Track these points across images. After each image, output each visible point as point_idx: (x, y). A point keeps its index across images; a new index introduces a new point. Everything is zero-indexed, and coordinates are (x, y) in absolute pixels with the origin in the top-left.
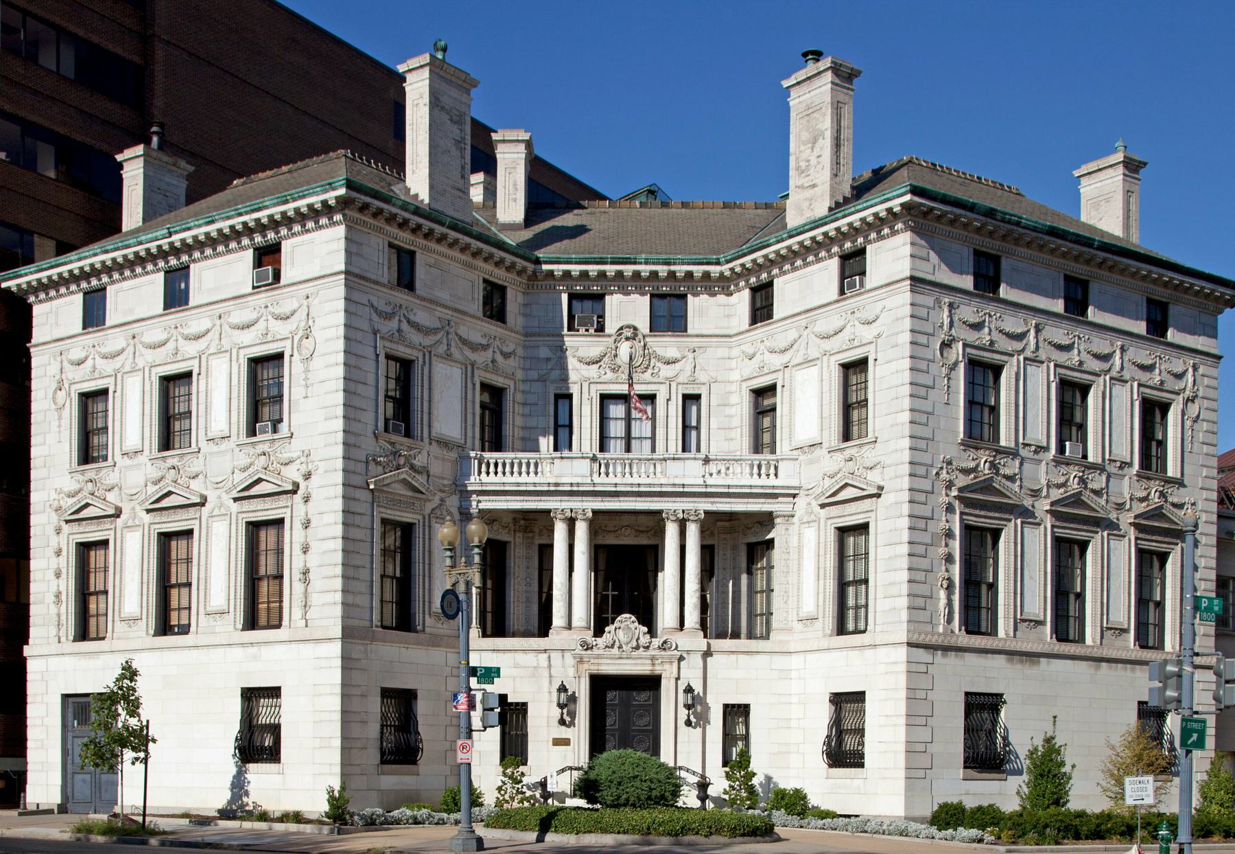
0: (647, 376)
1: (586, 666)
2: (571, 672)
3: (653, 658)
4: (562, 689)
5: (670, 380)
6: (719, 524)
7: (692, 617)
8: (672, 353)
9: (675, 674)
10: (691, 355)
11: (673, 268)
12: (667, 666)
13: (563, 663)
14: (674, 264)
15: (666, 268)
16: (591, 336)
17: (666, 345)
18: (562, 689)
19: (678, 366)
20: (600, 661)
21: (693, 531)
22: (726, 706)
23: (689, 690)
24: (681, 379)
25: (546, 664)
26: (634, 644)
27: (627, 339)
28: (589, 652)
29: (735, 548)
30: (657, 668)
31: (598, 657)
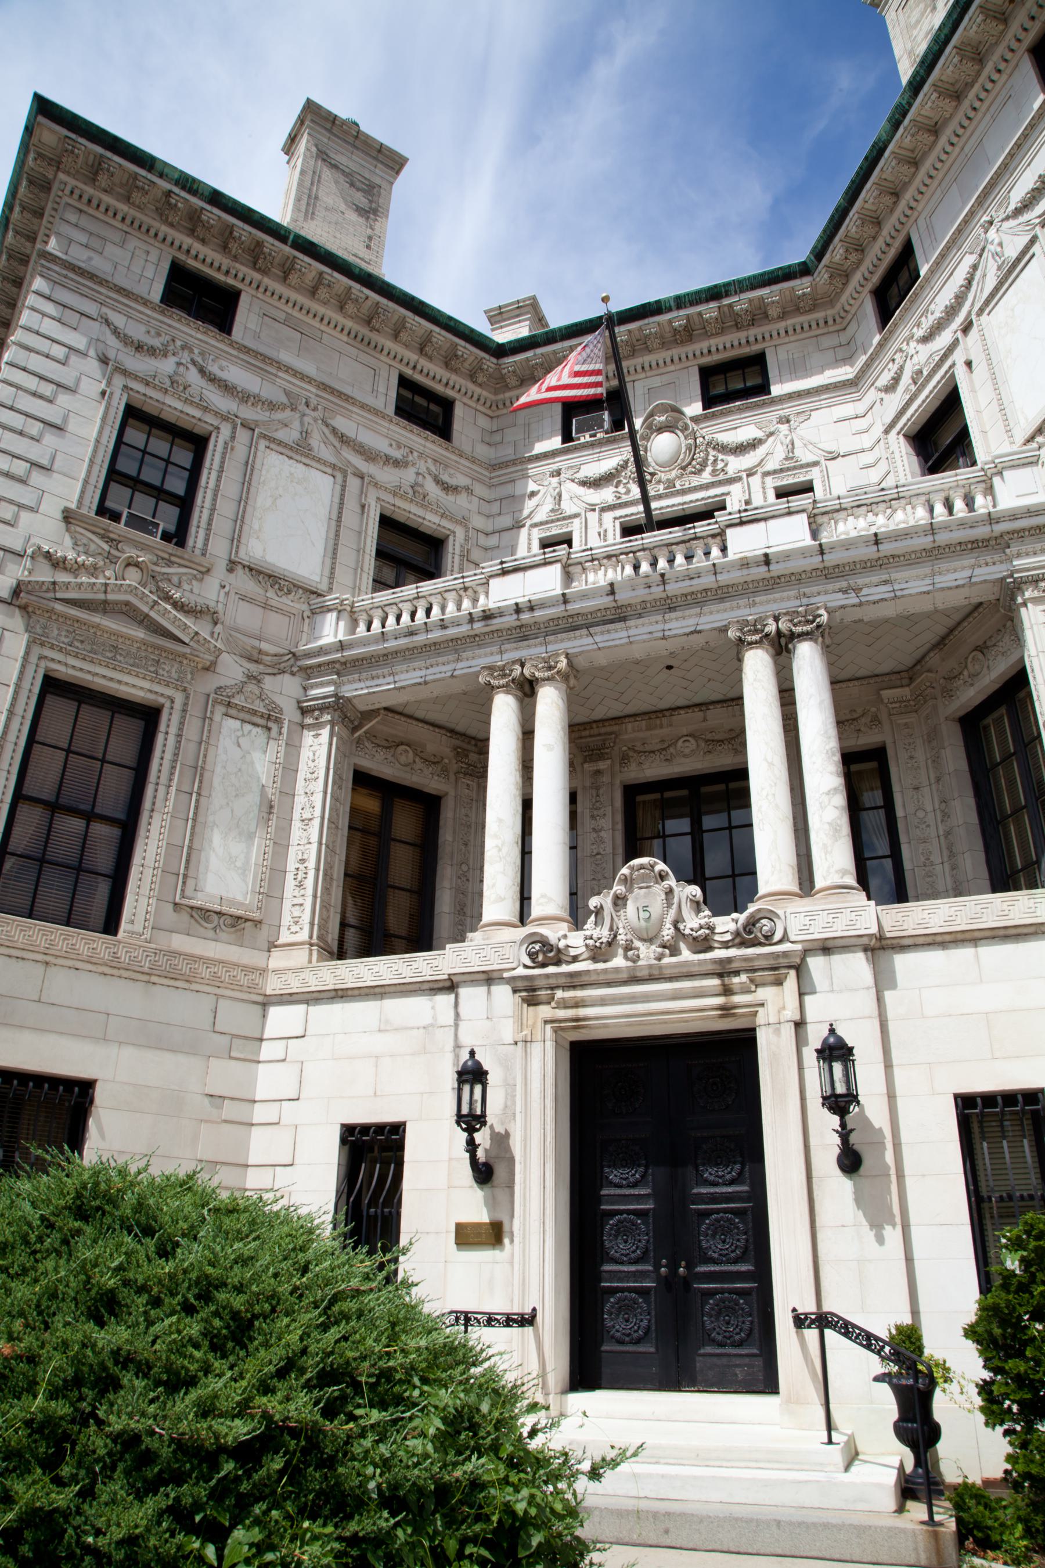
0: (706, 477)
1: (545, 1011)
2: (508, 1031)
3: (724, 971)
4: (472, 1074)
5: (750, 473)
6: (886, 694)
8: (746, 432)
9: (791, 1012)
10: (784, 428)
11: (726, 301)
12: (764, 993)
13: (489, 1007)
14: (727, 295)
15: (713, 305)
16: (600, 443)
17: (739, 426)
18: (472, 1074)
19: (761, 451)
21: (808, 663)
22: (965, 1103)
23: (836, 1051)
24: (771, 465)
25: (449, 1018)
26: (668, 932)
27: (660, 430)
28: (551, 969)
29: (932, 736)
30: (737, 999)
31: (574, 982)
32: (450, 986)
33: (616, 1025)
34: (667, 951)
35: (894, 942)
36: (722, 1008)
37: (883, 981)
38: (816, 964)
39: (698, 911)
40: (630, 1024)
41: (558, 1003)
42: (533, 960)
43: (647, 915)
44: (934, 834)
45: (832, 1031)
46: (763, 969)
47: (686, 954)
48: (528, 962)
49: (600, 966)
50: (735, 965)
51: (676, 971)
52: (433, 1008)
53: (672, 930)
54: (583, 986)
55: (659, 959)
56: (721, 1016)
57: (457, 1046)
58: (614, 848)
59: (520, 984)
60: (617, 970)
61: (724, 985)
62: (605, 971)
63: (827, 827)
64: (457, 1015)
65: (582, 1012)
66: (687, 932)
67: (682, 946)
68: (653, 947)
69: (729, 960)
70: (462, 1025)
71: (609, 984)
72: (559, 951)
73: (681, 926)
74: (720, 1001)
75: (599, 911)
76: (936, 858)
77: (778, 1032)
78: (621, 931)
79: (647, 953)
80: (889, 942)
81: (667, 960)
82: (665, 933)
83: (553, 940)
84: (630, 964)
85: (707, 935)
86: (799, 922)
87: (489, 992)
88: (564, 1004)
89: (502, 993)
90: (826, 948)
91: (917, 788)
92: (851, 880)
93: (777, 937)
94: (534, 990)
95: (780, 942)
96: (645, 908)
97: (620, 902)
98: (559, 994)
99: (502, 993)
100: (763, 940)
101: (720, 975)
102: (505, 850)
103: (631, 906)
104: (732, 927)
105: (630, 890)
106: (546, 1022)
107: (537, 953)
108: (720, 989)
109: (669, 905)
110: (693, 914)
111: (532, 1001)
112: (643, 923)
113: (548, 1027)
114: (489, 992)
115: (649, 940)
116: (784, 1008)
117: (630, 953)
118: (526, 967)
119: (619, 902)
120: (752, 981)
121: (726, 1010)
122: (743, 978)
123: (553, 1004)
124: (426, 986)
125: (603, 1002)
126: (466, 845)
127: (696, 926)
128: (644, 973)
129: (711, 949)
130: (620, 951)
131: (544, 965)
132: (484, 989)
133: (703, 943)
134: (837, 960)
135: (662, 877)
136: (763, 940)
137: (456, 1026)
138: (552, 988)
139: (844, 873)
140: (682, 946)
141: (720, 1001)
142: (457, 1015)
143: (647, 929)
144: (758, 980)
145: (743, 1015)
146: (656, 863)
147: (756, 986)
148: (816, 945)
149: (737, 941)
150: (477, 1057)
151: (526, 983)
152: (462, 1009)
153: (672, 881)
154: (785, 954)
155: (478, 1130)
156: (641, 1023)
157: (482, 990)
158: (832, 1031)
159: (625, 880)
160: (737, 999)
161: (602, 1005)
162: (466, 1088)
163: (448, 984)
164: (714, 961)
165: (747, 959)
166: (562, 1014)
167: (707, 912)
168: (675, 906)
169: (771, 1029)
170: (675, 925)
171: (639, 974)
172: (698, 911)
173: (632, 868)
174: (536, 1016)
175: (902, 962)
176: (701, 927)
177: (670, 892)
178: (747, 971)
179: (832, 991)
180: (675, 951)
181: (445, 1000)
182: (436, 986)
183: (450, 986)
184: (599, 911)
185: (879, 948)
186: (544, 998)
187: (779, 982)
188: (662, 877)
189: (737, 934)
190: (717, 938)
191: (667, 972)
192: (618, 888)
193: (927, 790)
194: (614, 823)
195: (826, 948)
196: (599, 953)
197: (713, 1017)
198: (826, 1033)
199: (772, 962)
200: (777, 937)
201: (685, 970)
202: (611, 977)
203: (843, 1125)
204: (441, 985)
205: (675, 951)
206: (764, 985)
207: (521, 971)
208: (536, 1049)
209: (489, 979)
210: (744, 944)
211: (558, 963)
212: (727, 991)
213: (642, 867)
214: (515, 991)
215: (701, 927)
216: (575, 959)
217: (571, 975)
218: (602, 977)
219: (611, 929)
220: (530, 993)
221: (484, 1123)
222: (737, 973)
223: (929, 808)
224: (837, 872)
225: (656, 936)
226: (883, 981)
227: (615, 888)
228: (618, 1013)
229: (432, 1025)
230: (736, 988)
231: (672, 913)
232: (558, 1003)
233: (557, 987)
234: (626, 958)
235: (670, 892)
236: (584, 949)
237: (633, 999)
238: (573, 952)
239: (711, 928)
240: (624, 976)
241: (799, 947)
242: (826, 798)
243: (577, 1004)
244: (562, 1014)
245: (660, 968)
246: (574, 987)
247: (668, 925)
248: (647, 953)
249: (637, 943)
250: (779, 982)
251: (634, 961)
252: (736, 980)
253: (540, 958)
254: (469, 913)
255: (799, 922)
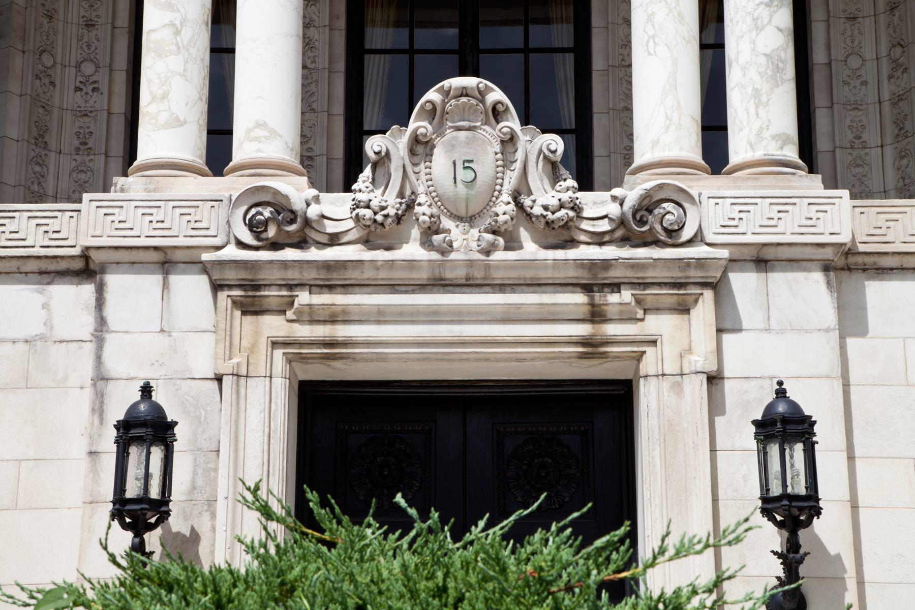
1: (274, 326)
3: (595, 282)
4: (147, 428)
7: (762, 115)
12: (656, 324)
18: (147, 428)
20: (339, 299)
23: (785, 426)
25: (85, 324)
26: (504, 208)
28: (290, 254)
30: (611, 330)
31: (333, 278)
32: (86, 268)
33: (399, 358)
34: (501, 241)
35: (869, 260)
36: (585, 342)
37: (851, 321)
38: (744, 284)
39: (555, 178)
40: (424, 358)
41: (299, 312)
42: (258, 236)
43: (470, 175)
44: (872, 97)
45: (781, 393)
46: (660, 285)
47: (530, 249)
48: (247, 237)
49: (381, 255)
50: (615, 274)
51: (514, 274)
52: (45, 306)
53: (512, 206)
54: (346, 287)
55: (488, 253)
56: (582, 356)
57: (101, 378)
58: (331, 62)
59: (231, 275)
60: (411, 264)
61: (592, 305)
62: (391, 264)
63: (763, 60)
64: (101, 322)
65: (342, 331)
66: (537, 210)
67: (524, 235)
68: (475, 232)
69: (606, 264)
70: (112, 342)
71: (393, 287)
72: (307, 222)
73: (527, 202)
74: (582, 330)
75: (383, 159)
76: (872, 137)
77: (678, 389)
78: (422, 199)
79: (465, 241)
80: (860, 259)
81: (499, 255)
82: (500, 209)
83: (298, 204)
84: (435, 256)
85: (571, 220)
86: (719, 213)
87: (165, 286)
88: (311, 316)
89: (191, 288)
90: (762, 259)
91: (852, 19)
92: (792, 153)
93: (686, 234)
94: (257, 287)
95: (690, 242)
96: (468, 164)
97: (420, 149)
98: (303, 298)
99: (191, 288)
100: (663, 237)
101: (587, 288)
102: (187, 34)
103: (440, 161)
104: (614, 210)
105: (440, 131)
106: (275, 344)
107: (266, 223)
108: (584, 311)
109: (507, 164)
110: (547, 186)
111: (251, 308)
112: (461, 189)
113: (279, 353)
114: (165, 286)
115: (469, 220)
116: (690, 350)
117: (437, 239)
118: (241, 244)
119: (421, 148)
120: (639, 302)
121: (592, 347)
122: (626, 295)
123: (290, 314)
124: (32, 266)
125: (380, 317)
126: (51, 18)
127: (554, 202)
128: (459, 274)
129: (571, 243)
130: (415, 233)
131: (275, 246)
132: (157, 279)
133: (560, 233)
134: (780, 281)
135: (497, 113)
136: (663, 237)
137: (99, 341)
138: (290, 287)
139: (785, 141)
140: (524, 235)
141: (582, 330)
142: (101, 322)
143: (467, 200)
144: (650, 302)
145: (619, 357)
146: (488, 90)
147: (646, 311)
148: (747, 253)
149: (619, 234)
150: (157, 397)
151: (243, 275)
152: (110, 311)
153: (513, 122)
154: (701, 263)
155: (152, 527)
156: (444, 358)
157: (154, 280)
158: (781, 393)
159: (432, 113)
160: (611, 330)
161: (378, 322)
162: (135, 452)
163: (79, 265)
164: (580, 264)
165: (635, 265)
166: (304, 331)
167: (571, 183)
168: (518, 166)
169: (666, 384)
170: (516, 197)
171: (449, 275)
172: (555, 178)
173: (446, 93)
174: (257, 333)
175: (879, 294)
176: (562, 206)
177: (509, 141)
178: (632, 285)
179: (768, 330)
180: (512, 244)
181: (73, 297)
182: (52, 266)
183: (86, 268)
184: (383, 159)
185: (847, 266)
186: (273, 303)
187: (684, 309)
188: (497, 113)
189: (622, 222)
190: (585, 225)
191: (499, 276)
192: (417, 124)
193: (868, 22)
194: (333, 17)
195: (762, 259)
196: (376, 232)
197: (569, 356)
198: (770, 397)
199: (677, 274)
200: (686, 234)
201: (529, 274)
202: (399, 275)
203: (793, 545)
204: (63, 265)
205: (512, 244)
206: (658, 310)
207: (231, 252)
208: (256, 390)
209: (165, 261)
210: (627, 240)
211: (301, 243)
212: (596, 315)
213: (464, 92)
214: (217, 287)
215: (562, 206)
216: (334, 240)
217: (329, 266)
218: (383, 274)
219: (401, 195)
220: (247, 293)
221: (164, 516)
222: (616, 287)
223: (869, 54)
224: (774, 137)
225: (480, 214)
226: (851, 321)
227: (412, 125)
228: (403, 337)
229: (42, 338)
230: (611, 312)
231: (511, 179)
232: (299, 312)
233: (301, 285)
234: (426, 243)
235: (509, 141)
236: (350, 224)
237: (434, 316)
238: (331, 228)
239: (576, 208)
240: (423, 275)
241: (724, 253)
242: (764, 12)
243: (334, 318)
244: (304, 331)
245: (487, 267)
246: (331, 288)
247: (506, 197)
248: (465, 241)
249: (447, 223)
250: (684, 309)
251: (443, 253)
252: (613, 298)
253: (272, 232)
254: (53, 145)
255: (719, 213)
